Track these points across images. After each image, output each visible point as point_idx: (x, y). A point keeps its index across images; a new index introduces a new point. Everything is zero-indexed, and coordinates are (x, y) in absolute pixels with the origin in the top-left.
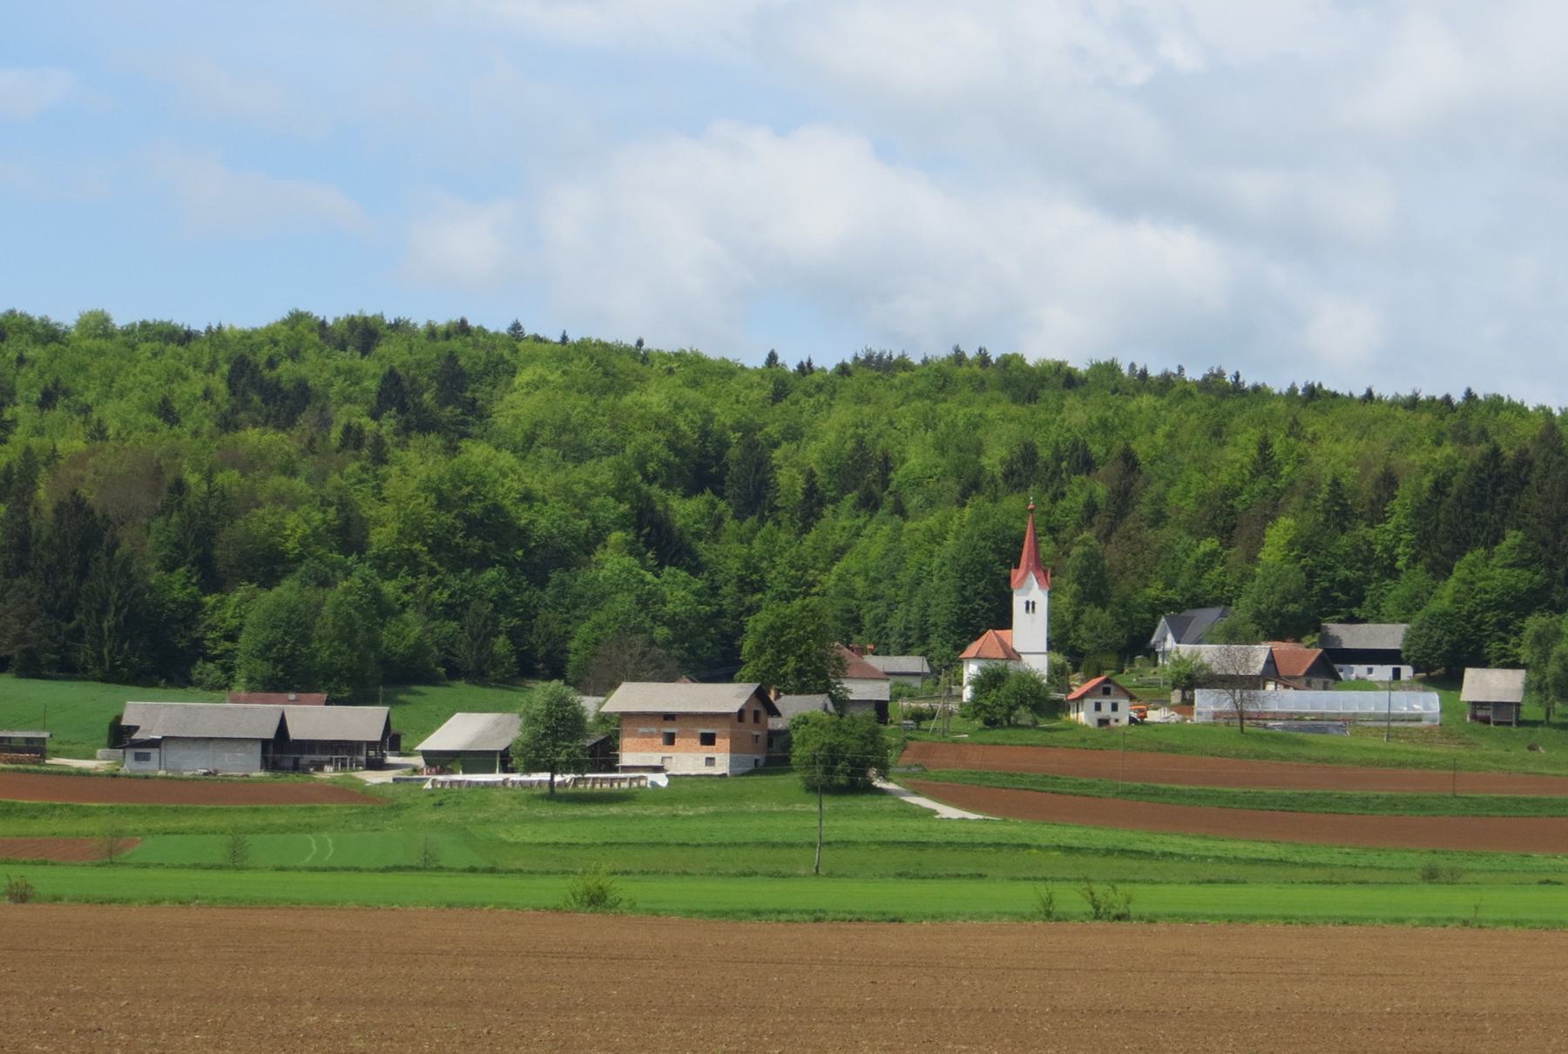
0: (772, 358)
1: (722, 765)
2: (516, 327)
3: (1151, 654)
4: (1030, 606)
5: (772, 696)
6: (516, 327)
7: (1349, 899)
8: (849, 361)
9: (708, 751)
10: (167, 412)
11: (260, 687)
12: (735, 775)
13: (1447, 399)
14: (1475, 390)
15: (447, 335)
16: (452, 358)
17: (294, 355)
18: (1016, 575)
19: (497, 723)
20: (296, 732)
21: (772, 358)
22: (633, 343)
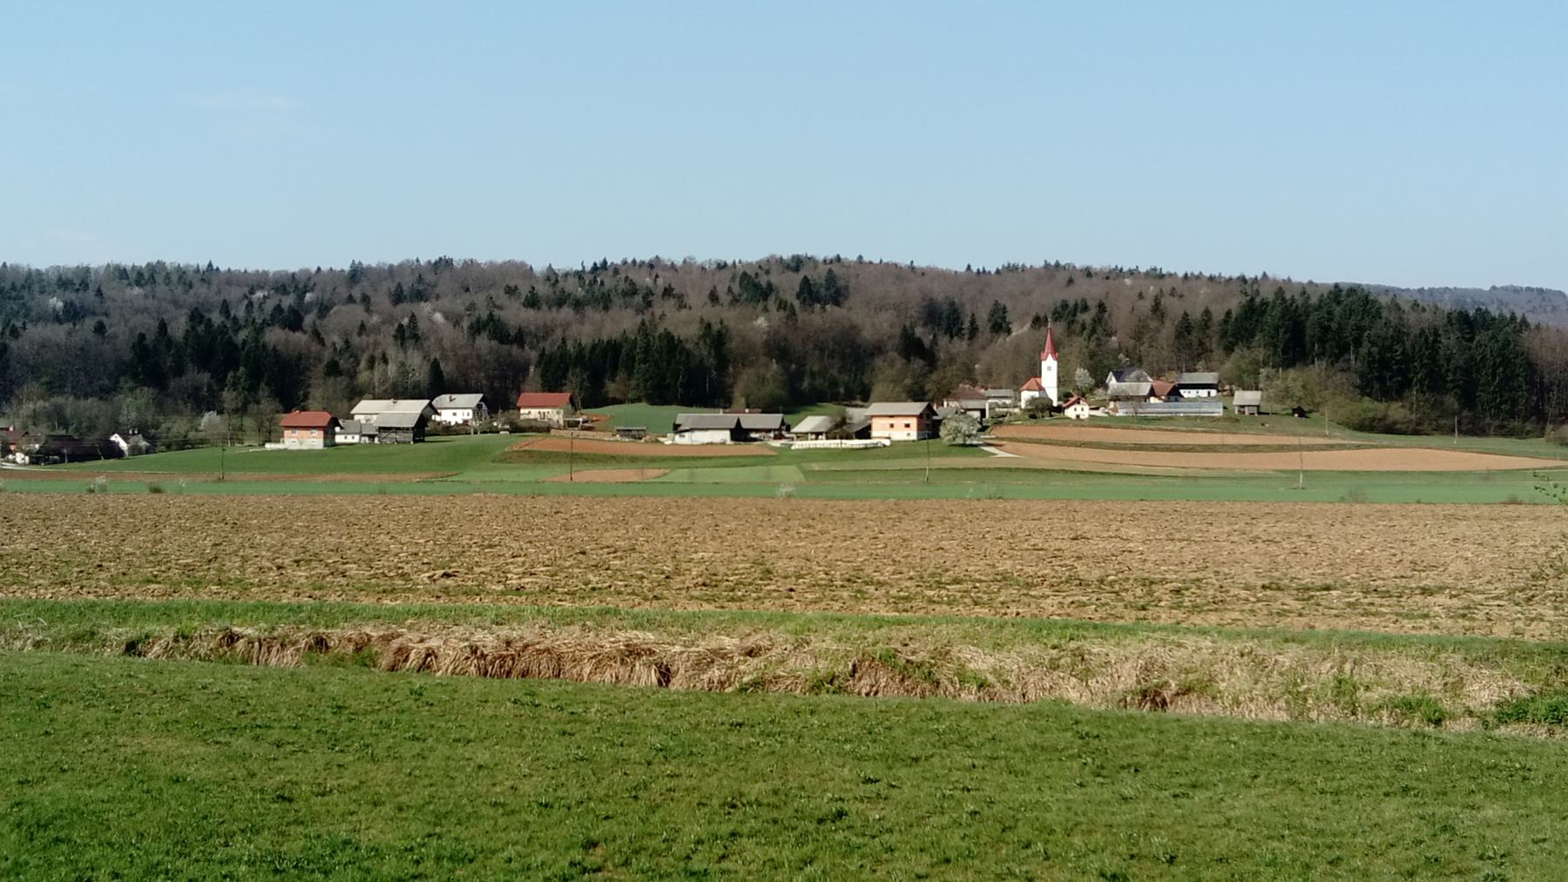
0: (969, 267)
1: (914, 436)
2: (860, 257)
3: (1106, 387)
4: (1049, 369)
5: (935, 408)
6: (860, 257)
7: (1289, 461)
8: (1000, 268)
9: (908, 430)
10: (1141, 296)
11: (904, 395)
12: (919, 440)
13: (1256, 278)
14: (1268, 273)
15: (831, 261)
16: (830, 271)
17: (767, 272)
18: (1043, 355)
19: (825, 420)
20: (745, 425)
21: (969, 267)
22: (909, 263)
